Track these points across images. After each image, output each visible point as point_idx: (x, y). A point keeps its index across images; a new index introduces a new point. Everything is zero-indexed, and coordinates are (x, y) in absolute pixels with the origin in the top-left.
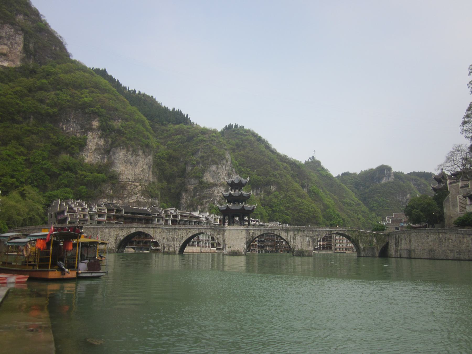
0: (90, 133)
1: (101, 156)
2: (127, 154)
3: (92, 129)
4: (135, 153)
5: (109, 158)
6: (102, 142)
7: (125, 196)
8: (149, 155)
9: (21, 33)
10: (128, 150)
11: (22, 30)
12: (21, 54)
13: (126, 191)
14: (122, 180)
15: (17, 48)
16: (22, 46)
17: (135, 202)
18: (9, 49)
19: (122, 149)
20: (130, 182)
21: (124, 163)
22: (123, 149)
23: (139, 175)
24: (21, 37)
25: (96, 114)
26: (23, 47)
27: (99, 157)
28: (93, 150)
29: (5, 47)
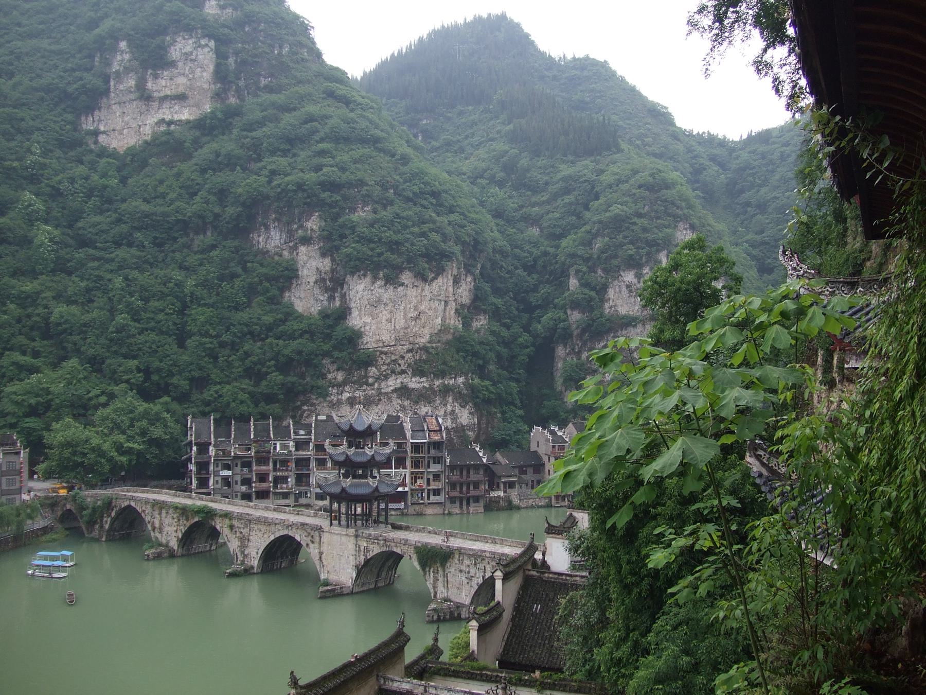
0: (303, 249)
1: (326, 295)
2: (372, 288)
3: (306, 241)
4: (392, 280)
5: (343, 296)
6: (326, 264)
7: (371, 380)
8: (435, 278)
9: (207, 42)
10: (375, 278)
11: (210, 36)
12: (213, 86)
13: (374, 369)
14: (366, 346)
15: (202, 77)
16: (211, 68)
17: (395, 390)
18: (188, 83)
19: (362, 277)
20: (384, 346)
21: (368, 306)
22: (365, 275)
23: (406, 328)
24: (207, 49)
25: (312, 204)
26: (214, 71)
27: (322, 298)
28: (312, 284)
29: (182, 80)
